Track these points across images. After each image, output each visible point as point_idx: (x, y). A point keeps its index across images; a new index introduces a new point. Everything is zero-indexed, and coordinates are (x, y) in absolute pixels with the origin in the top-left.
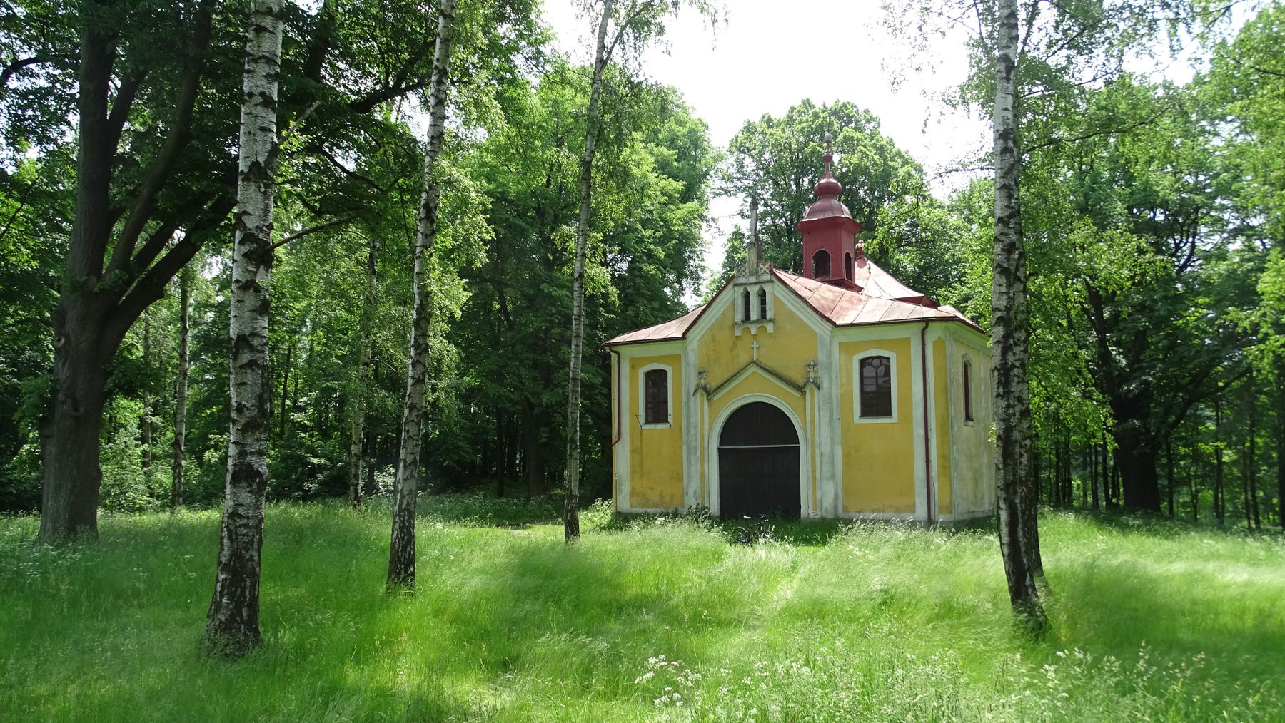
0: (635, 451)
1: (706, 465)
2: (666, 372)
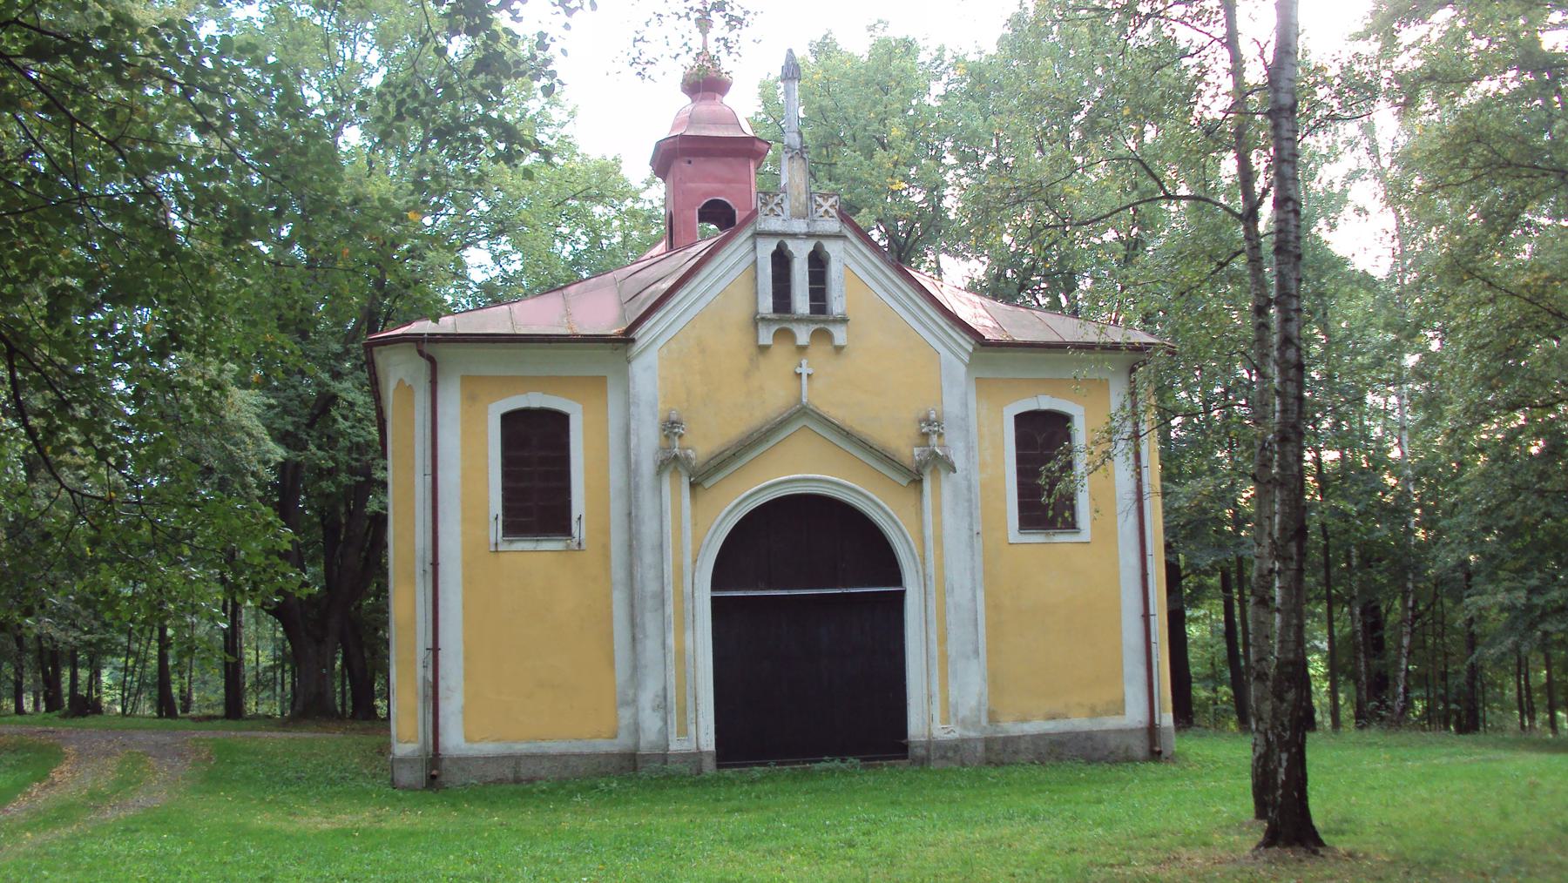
1: (689, 635)
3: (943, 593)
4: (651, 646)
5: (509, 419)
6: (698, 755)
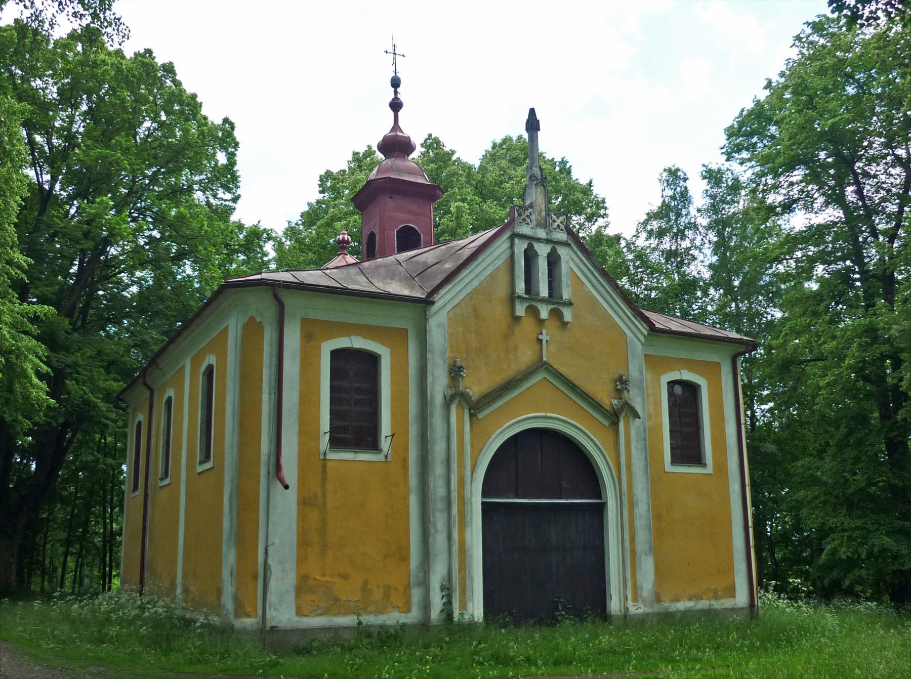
2: (373, 359)
4: (439, 540)
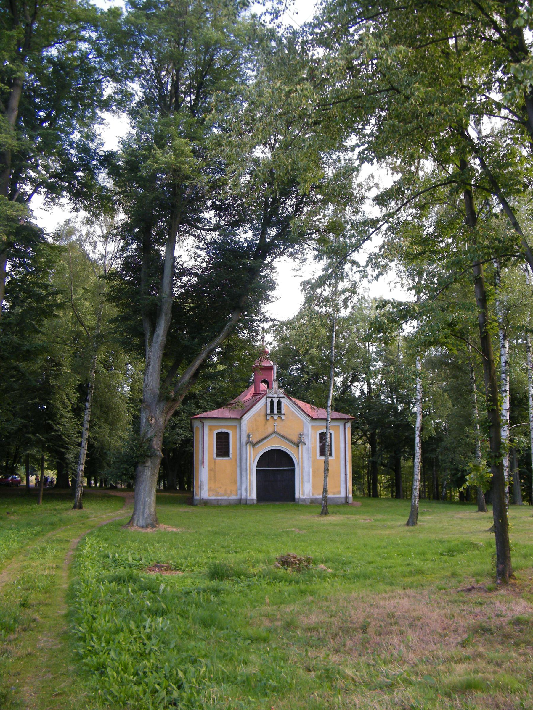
0: (210, 470)
2: (228, 434)
3: (303, 468)
4: (244, 479)
5: (218, 434)
6: (253, 500)
